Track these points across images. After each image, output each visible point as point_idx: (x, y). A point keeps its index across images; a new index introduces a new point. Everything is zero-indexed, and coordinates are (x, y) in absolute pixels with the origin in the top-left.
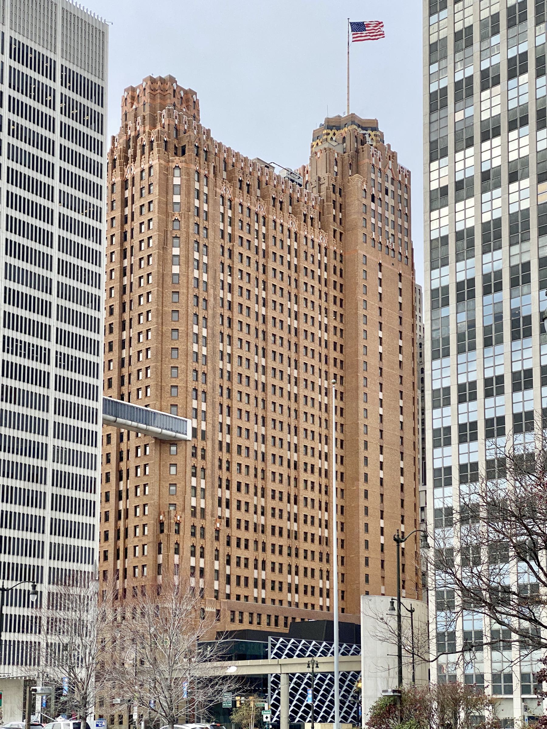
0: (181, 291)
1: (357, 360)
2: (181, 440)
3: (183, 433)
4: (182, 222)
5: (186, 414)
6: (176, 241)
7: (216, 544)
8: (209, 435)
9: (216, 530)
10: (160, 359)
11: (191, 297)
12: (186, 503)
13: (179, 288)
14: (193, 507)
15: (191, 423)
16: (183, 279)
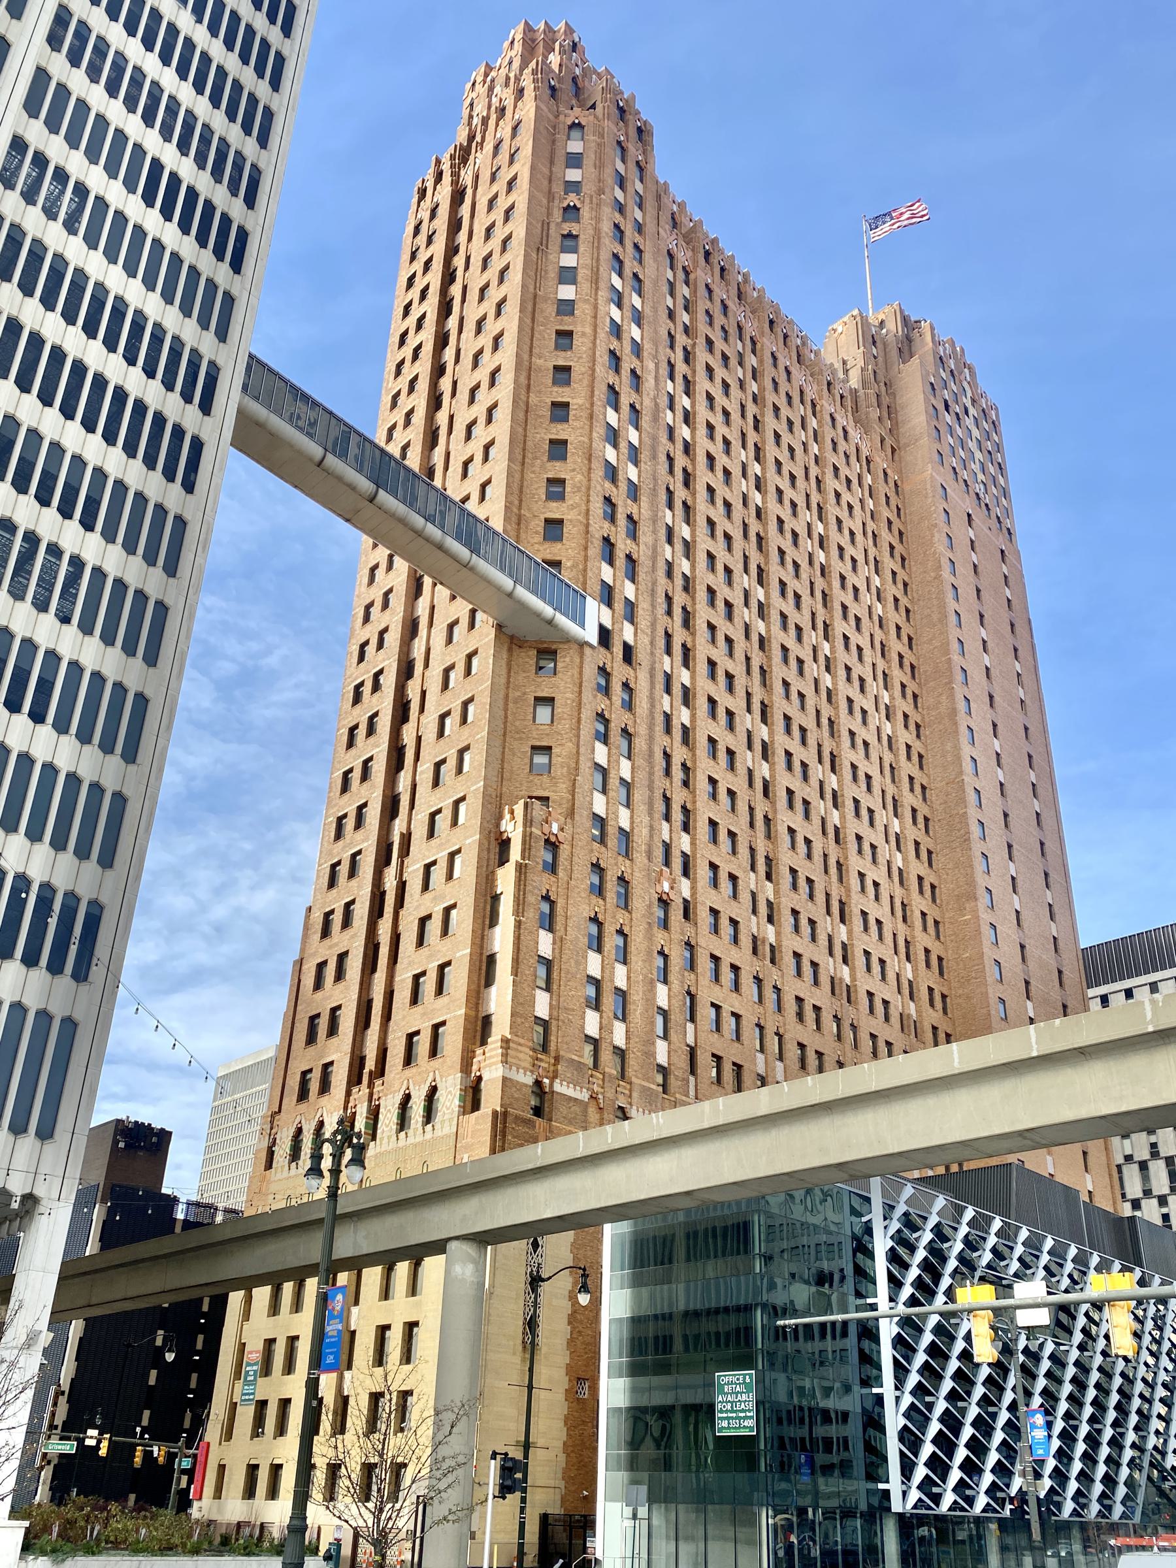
2: (568, 639)
3: (574, 620)
5: (584, 583)
7: (660, 937)
8: (641, 655)
9: (660, 900)
15: (596, 614)
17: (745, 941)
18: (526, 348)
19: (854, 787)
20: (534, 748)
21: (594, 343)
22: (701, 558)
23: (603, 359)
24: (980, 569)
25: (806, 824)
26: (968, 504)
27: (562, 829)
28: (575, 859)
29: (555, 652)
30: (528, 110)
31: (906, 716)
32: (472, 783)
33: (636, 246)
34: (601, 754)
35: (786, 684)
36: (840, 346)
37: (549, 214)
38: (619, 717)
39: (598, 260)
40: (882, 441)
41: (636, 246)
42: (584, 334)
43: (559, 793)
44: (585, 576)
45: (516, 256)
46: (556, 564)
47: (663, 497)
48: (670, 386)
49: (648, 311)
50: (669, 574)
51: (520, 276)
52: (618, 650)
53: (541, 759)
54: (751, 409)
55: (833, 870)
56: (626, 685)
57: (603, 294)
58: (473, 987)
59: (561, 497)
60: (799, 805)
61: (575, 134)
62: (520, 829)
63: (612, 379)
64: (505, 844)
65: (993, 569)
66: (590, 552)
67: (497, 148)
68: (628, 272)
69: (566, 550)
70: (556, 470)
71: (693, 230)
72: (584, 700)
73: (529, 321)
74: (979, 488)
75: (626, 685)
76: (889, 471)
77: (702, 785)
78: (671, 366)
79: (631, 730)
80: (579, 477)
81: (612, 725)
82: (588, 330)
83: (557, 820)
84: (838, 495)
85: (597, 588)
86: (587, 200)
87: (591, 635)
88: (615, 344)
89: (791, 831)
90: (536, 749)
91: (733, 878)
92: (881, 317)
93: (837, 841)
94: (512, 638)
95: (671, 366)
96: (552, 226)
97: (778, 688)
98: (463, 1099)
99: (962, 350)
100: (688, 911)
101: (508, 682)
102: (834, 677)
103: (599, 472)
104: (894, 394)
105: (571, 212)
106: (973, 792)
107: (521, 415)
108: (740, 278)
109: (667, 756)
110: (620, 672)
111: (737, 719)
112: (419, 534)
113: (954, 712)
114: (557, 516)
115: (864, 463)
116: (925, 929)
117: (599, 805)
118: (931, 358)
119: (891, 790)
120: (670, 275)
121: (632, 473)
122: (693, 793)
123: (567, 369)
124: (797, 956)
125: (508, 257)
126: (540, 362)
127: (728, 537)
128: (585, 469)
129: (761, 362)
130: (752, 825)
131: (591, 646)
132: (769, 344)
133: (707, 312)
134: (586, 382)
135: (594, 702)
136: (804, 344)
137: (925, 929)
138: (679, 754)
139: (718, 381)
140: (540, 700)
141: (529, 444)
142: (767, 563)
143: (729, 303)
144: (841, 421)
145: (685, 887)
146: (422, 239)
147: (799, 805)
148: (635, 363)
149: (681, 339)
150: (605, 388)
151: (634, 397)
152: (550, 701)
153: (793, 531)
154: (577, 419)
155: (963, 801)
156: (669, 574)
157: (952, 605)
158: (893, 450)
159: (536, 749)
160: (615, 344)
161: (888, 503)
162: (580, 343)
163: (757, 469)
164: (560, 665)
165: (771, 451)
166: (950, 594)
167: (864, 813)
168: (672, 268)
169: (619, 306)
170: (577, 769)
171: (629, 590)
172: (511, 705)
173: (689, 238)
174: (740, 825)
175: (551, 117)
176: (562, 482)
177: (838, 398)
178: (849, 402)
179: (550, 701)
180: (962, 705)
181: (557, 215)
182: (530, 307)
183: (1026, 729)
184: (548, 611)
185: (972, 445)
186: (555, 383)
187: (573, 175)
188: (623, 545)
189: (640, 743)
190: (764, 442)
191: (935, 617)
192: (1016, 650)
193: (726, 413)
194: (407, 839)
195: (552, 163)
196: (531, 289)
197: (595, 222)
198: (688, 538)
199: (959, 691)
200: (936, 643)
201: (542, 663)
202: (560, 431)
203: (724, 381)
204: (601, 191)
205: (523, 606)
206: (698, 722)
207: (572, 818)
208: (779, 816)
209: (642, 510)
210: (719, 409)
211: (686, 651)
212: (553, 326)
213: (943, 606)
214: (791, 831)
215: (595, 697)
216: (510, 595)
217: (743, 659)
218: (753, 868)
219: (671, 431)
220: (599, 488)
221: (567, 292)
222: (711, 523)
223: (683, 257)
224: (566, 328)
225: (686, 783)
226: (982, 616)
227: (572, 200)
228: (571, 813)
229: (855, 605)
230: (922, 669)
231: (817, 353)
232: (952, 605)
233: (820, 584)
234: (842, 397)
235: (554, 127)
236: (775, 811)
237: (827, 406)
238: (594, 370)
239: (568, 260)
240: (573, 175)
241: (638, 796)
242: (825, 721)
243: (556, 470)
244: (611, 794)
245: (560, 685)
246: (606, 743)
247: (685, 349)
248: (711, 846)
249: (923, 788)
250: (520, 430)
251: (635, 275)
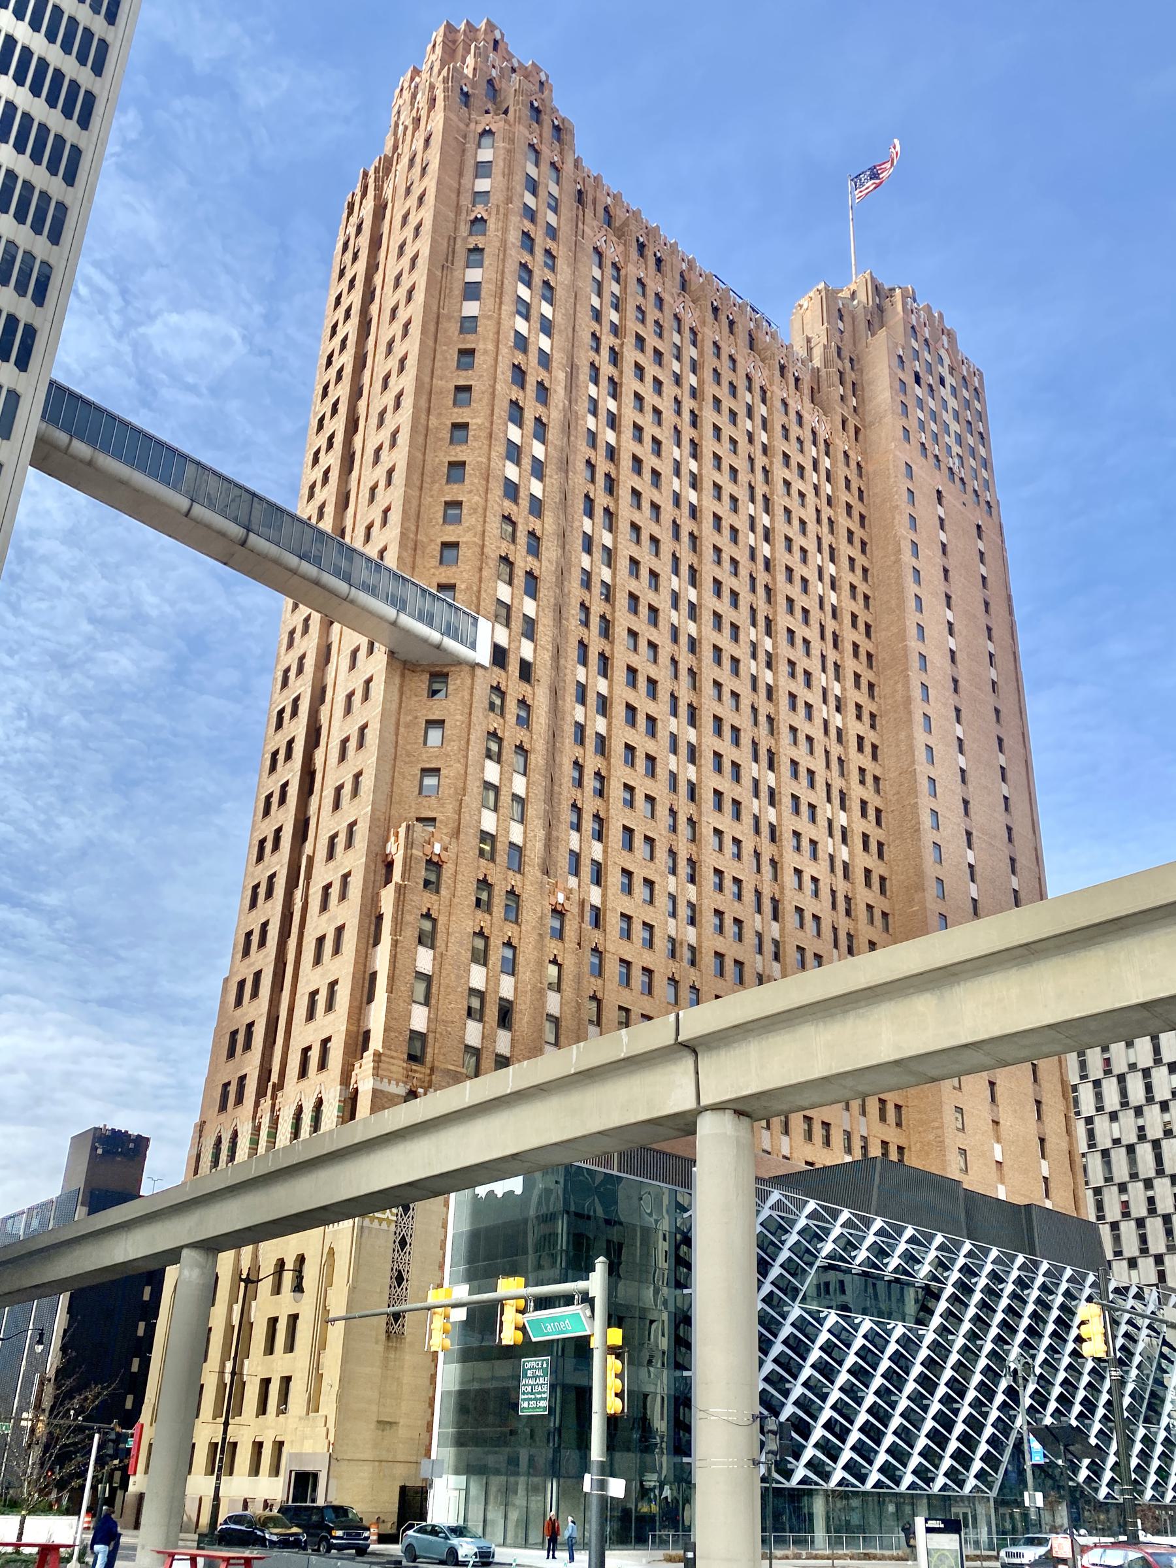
0: (480, 347)
1: (905, 648)
2: (459, 662)
12: (466, 818)
15: (488, 634)
17: (661, 943)
18: (428, 371)
19: (794, 783)
20: (423, 770)
21: (496, 360)
22: (623, 564)
23: (505, 373)
24: (949, 549)
25: (735, 824)
26: (940, 481)
27: (446, 849)
28: (459, 877)
29: (446, 675)
30: (436, 122)
31: (859, 707)
32: (360, 810)
33: (548, 252)
34: (492, 772)
35: (718, 685)
36: (803, 327)
37: (456, 229)
38: (512, 734)
39: (503, 273)
40: (844, 422)
41: (548, 252)
42: (485, 352)
43: (444, 813)
44: (478, 598)
45: (420, 277)
46: (450, 587)
47: (580, 505)
48: (593, 390)
49: (560, 321)
50: (587, 584)
51: (422, 295)
52: (514, 667)
53: (430, 781)
54: (688, 404)
55: (766, 868)
56: (522, 703)
57: (508, 307)
58: (356, 1004)
59: (458, 520)
60: (727, 806)
61: (486, 141)
62: (401, 852)
63: (515, 394)
64: (390, 865)
65: (964, 547)
66: (485, 573)
67: (412, 161)
68: (537, 281)
69: (462, 574)
70: (454, 492)
71: (626, 223)
72: (474, 719)
73: (431, 343)
74: (954, 463)
75: (522, 703)
76: (851, 454)
77: (616, 792)
78: (594, 368)
79: (526, 746)
80: (476, 498)
81: (505, 743)
82: (490, 347)
83: (440, 840)
84: (787, 484)
85: (492, 608)
86: (494, 211)
87: (483, 655)
88: (519, 358)
89: (718, 832)
90: (426, 771)
91: (649, 883)
92: (853, 287)
93: (773, 839)
94: (405, 663)
95: (594, 368)
96: (459, 241)
97: (708, 689)
98: (340, 1109)
99: (941, 315)
100: (598, 917)
101: (400, 707)
102: (775, 674)
103: (497, 490)
104: (861, 371)
105: (478, 223)
106: (926, 782)
107: (421, 440)
108: (684, 266)
109: (578, 766)
110: (515, 688)
111: (659, 724)
112: (294, 572)
113: (908, 700)
114: (453, 539)
115: (822, 446)
116: (872, 922)
117: (489, 821)
118: (901, 329)
119: (837, 783)
120: (597, 273)
121: (536, 488)
123: (468, 389)
124: (719, 956)
125: (415, 275)
127: (654, 540)
128: (482, 490)
129: (701, 354)
130: (674, 829)
131: (482, 666)
132: (711, 333)
133: (639, 308)
134: (485, 401)
135: (484, 721)
136: (758, 327)
137: (872, 922)
138: (592, 763)
139: (648, 379)
140: (431, 723)
141: (428, 468)
142: (700, 562)
143: (666, 297)
144: (794, 405)
145: (595, 896)
146: (349, 255)
147: (727, 806)
148: (543, 375)
149: (608, 340)
150: (506, 405)
151: (540, 410)
152: (440, 723)
153: (732, 527)
154: (476, 438)
155: (913, 791)
156: (587, 584)
157: (912, 588)
158: (857, 430)
159: (426, 771)
160: (519, 358)
161: (848, 487)
162: (481, 361)
163: (693, 466)
164: (451, 687)
165: (709, 446)
166: (909, 577)
167: (804, 808)
168: (600, 267)
169: (527, 318)
170: (464, 789)
171: (529, 607)
172: (402, 730)
173: (620, 233)
174: (659, 829)
175: (462, 126)
176: (458, 504)
177: (792, 381)
178: (805, 387)
179: (440, 723)
180: (917, 693)
181: (464, 229)
182: (432, 328)
183: (997, 711)
184: (435, 636)
185: (948, 417)
186: (455, 404)
187: (483, 185)
188: (523, 562)
189: (537, 759)
190: (701, 437)
191: (893, 603)
192: (989, 629)
193: (657, 412)
194: (311, 859)
195: (461, 175)
196: (435, 308)
197: (502, 234)
198: (609, 545)
199: (916, 677)
200: (894, 630)
201: (436, 687)
202: (459, 453)
203: (655, 379)
204: (509, 200)
205: (408, 633)
206: (614, 731)
207: (458, 838)
208: (704, 819)
209: (548, 526)
210: (648, 408)
211: (604, 659)
212: (453, 346)
213: (901, 590)
214: (718, 832)
215: (486, 717)
216: (394, 624)
217: (668, 662)
218: (673, 871)
219: (592, 437)
220: (496, 507)
221: (471, 308)
222: (635, 527)
223: (612, 253)
224: (468, 346)
225: (600, 793)
226: (948, 597)
227: (480, 211)
228: (457, 833)
229: (804, 597)
230: (881, 657)
231: (774, 336)
232: (912, 588)
233: (762, 578)
234: (797, 380)
235: (465, 137)
236: (700, 814)
237: (778, 392)
238: (494, 387)
239: (474, 275)
240: (483, 185)
241: (531, 811)
242: (762, 719)
243: (454, 492)
244: (501, 810)
245: (448, 706)
246: (499, 762)
247: (612, 349)
248: (625, 853)
249: (876, 779)
250: (419, 455)
251: (546, 283)
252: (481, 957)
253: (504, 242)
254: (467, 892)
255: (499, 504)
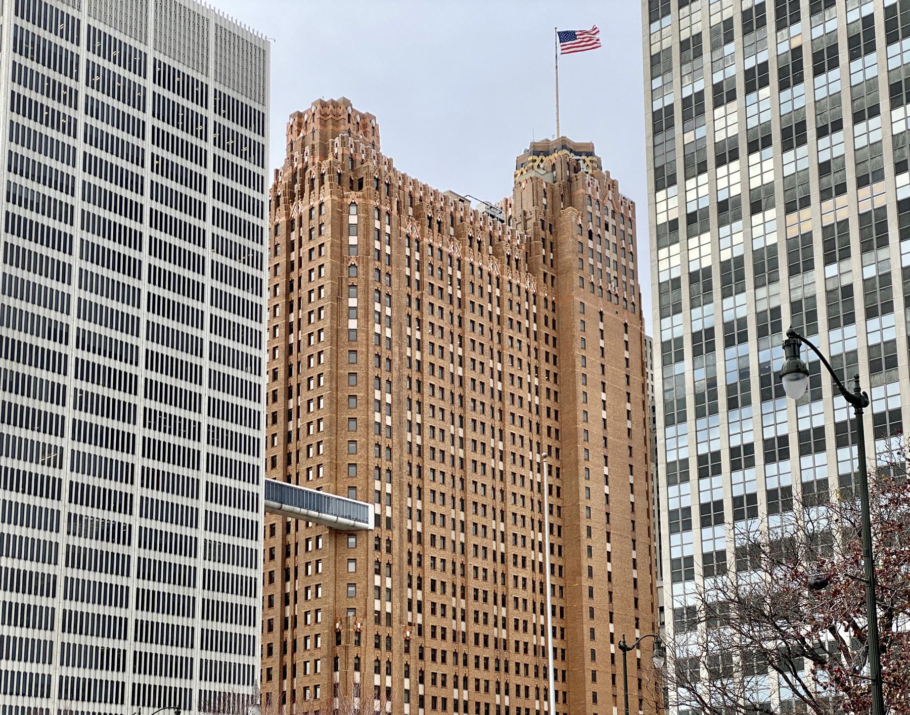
0: (359, 349)
2: (361, 530)
3: (363, 521)
4: (360, 268)
5: (367, 498)
6: (353, 290)
7: (406, 658)
8: (395, 522)
9: (406, 640)
10: (335, 431)
11: (371, 357)
13: (357, 346)
14: (376, 612)
15: (373, 509)
16: (361, 336)
43: (359, 606)
44: (367, 493)
80: (363, 439)
122: (423, 569)
126: (342, 371)
184: (352, 522)
252: (377, 670)
253: (367, 280)
254: (371, 642)
255: (373, 438)
